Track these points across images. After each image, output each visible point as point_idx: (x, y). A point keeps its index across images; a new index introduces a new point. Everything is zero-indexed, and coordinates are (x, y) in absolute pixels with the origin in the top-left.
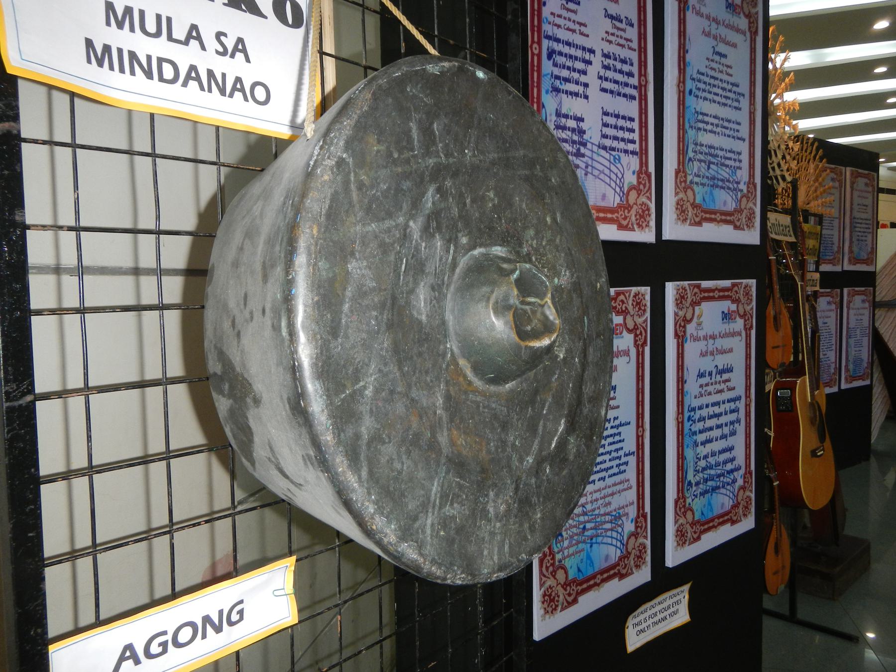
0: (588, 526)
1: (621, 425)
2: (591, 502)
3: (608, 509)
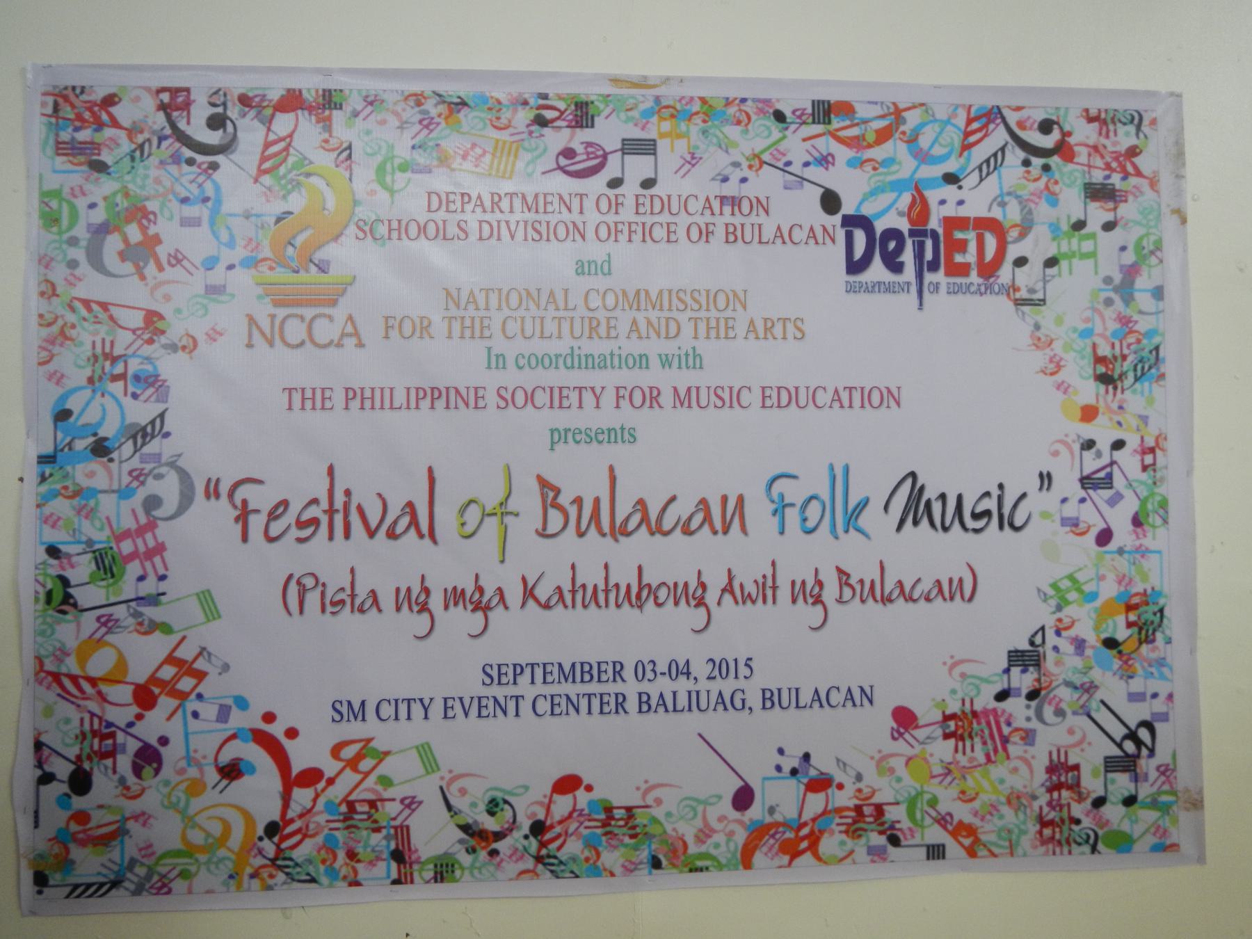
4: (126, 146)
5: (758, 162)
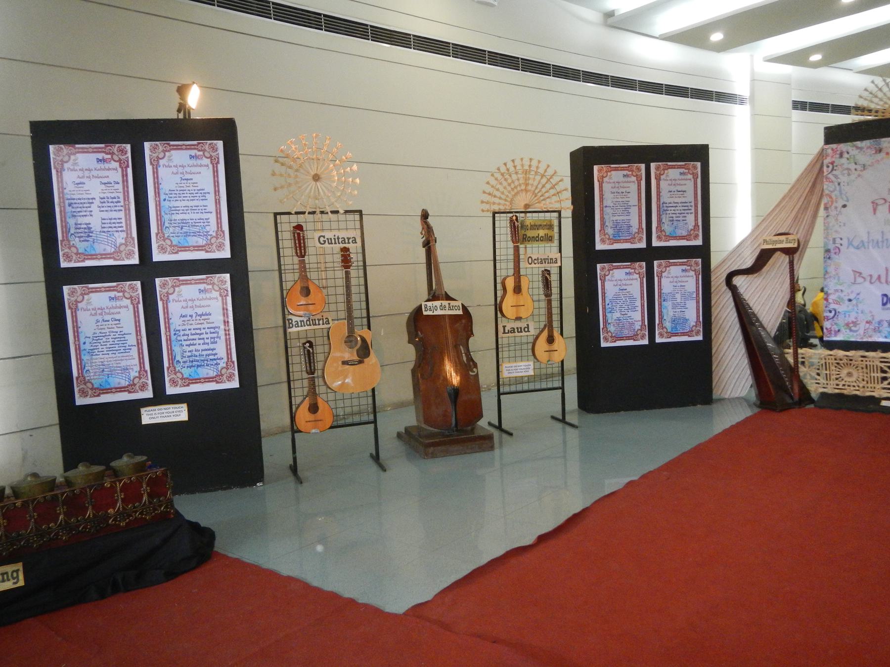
0: (105, 370)
1: (125, 334)
2: (107, 361)
3: (119, 365)
4: (835, 326)
5: (837, 220)
